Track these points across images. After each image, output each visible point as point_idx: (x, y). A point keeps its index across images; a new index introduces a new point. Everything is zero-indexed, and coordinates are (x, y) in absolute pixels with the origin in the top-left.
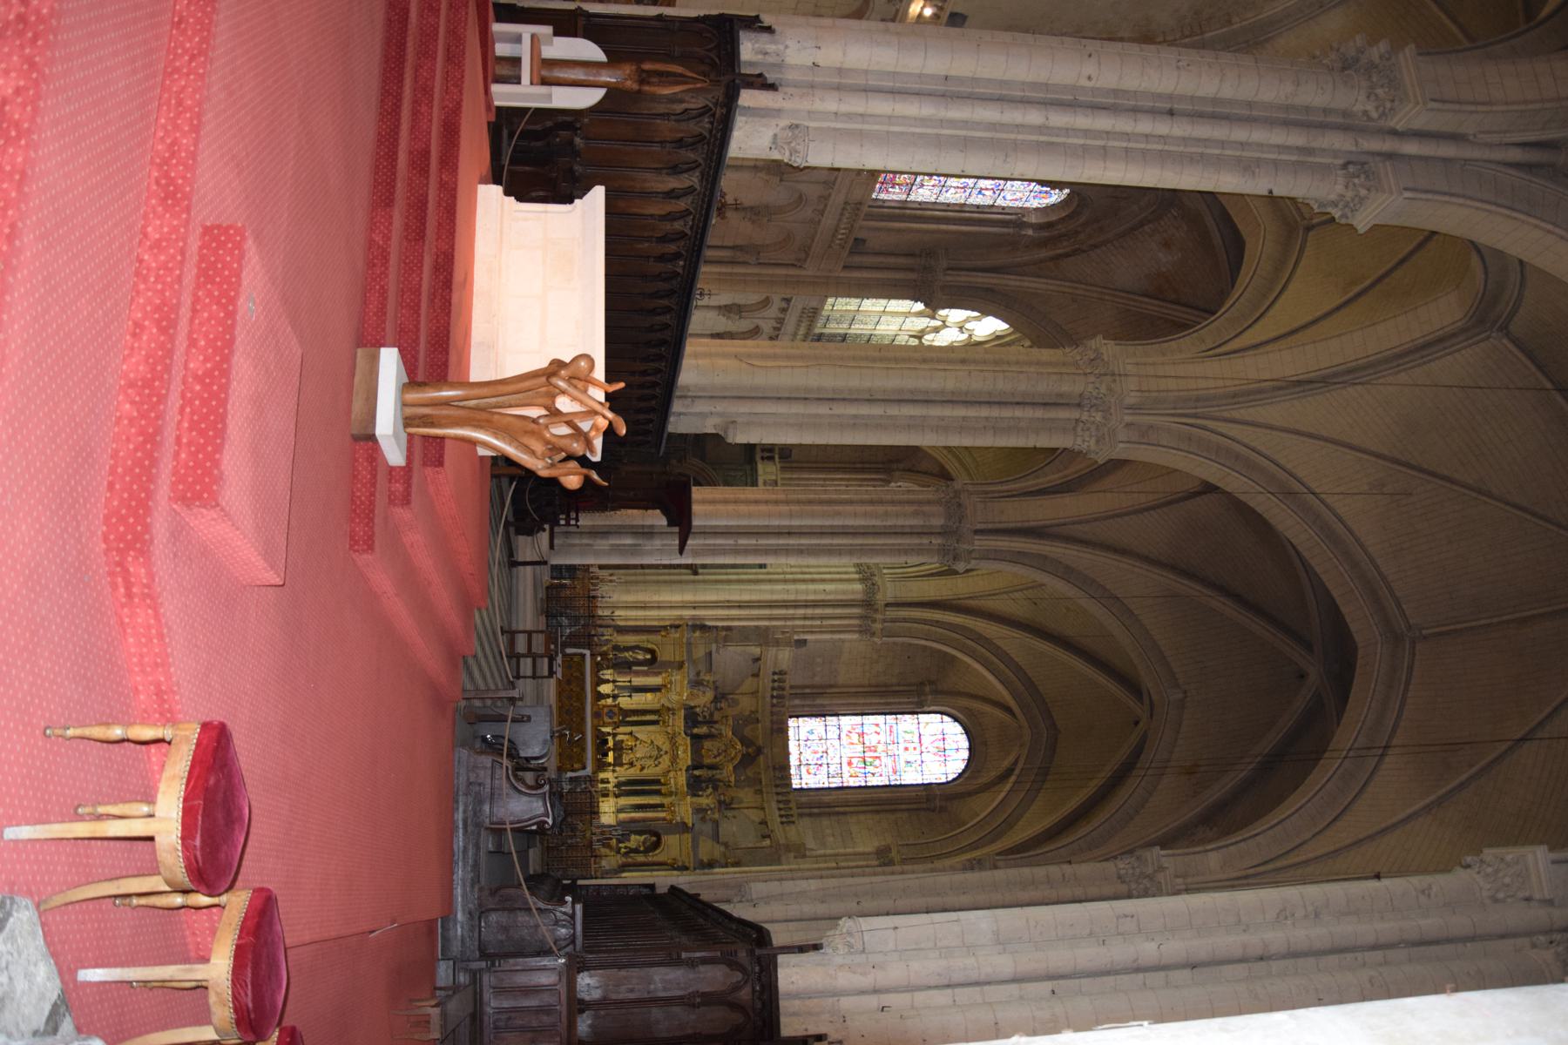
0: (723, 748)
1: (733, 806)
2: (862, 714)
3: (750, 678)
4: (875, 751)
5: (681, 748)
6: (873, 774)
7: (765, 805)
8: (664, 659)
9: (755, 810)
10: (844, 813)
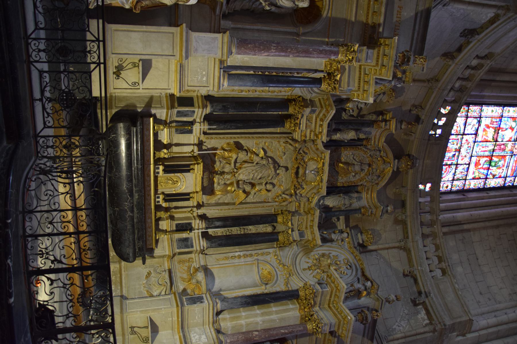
0: (367, 161)
1: (371, 248)
2: (504, 105)
3: (438, 59)
4: (504, 150)
5: (312, 166)
6: (494, 176)
7: (410, 245)
8: (336, 14)
9: (396, 251)
10: (468, 230)
